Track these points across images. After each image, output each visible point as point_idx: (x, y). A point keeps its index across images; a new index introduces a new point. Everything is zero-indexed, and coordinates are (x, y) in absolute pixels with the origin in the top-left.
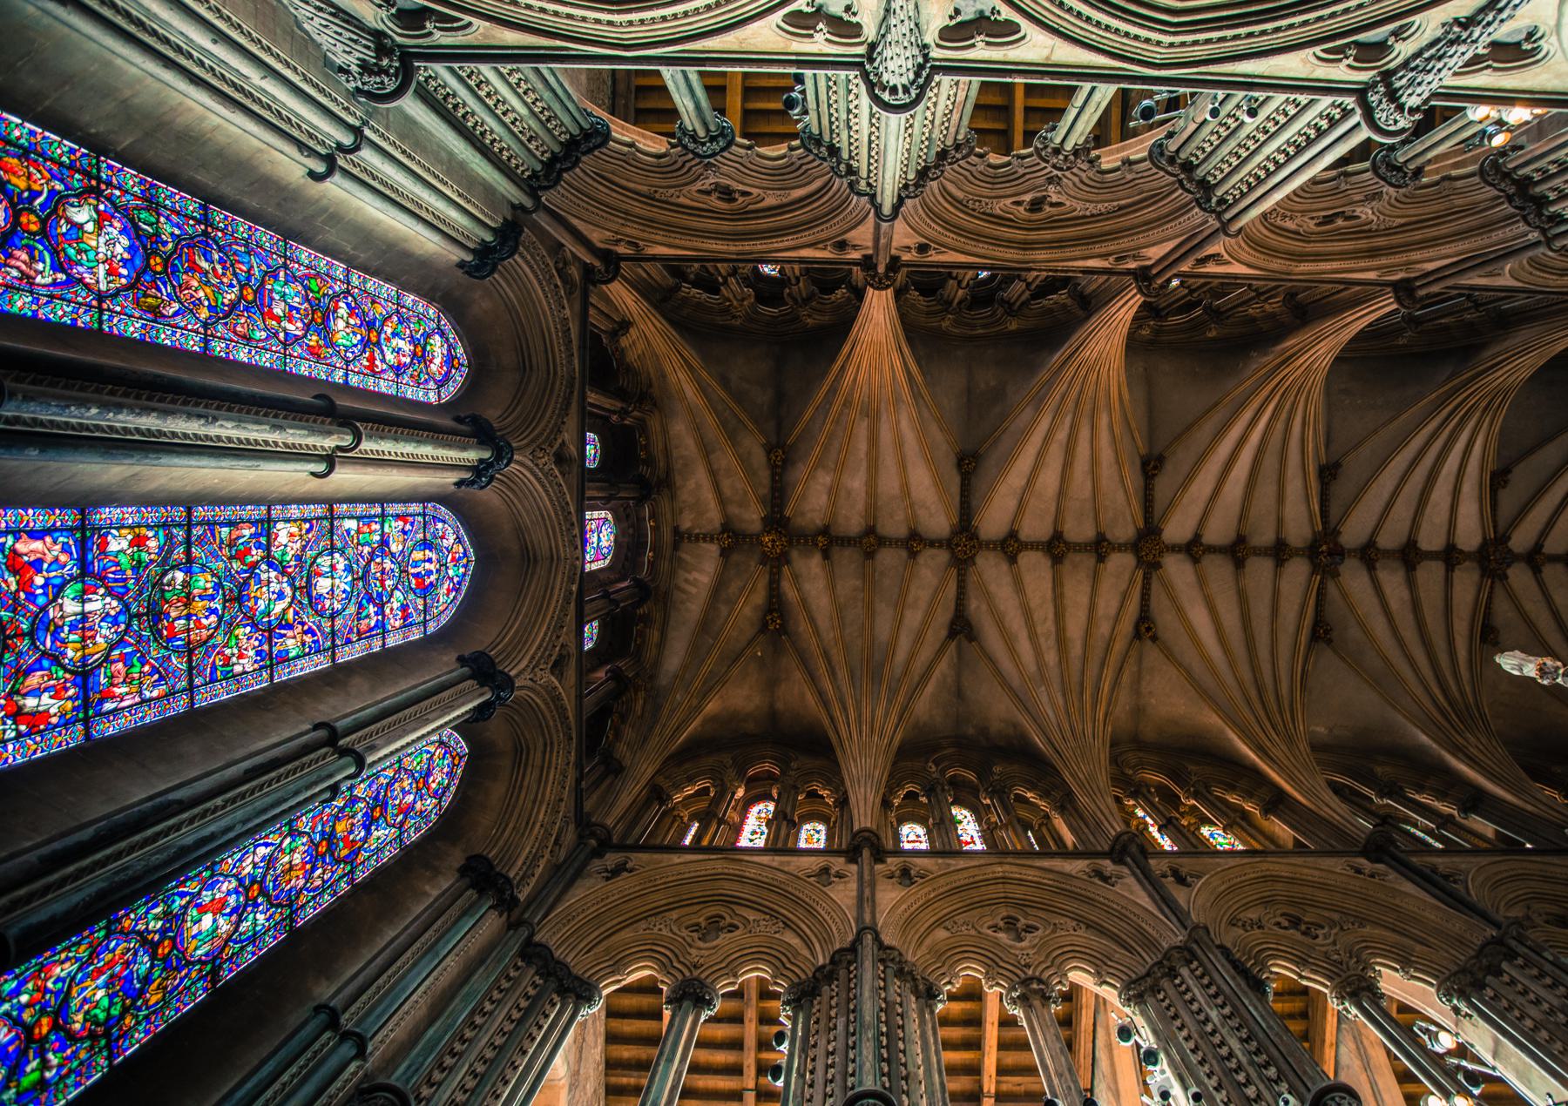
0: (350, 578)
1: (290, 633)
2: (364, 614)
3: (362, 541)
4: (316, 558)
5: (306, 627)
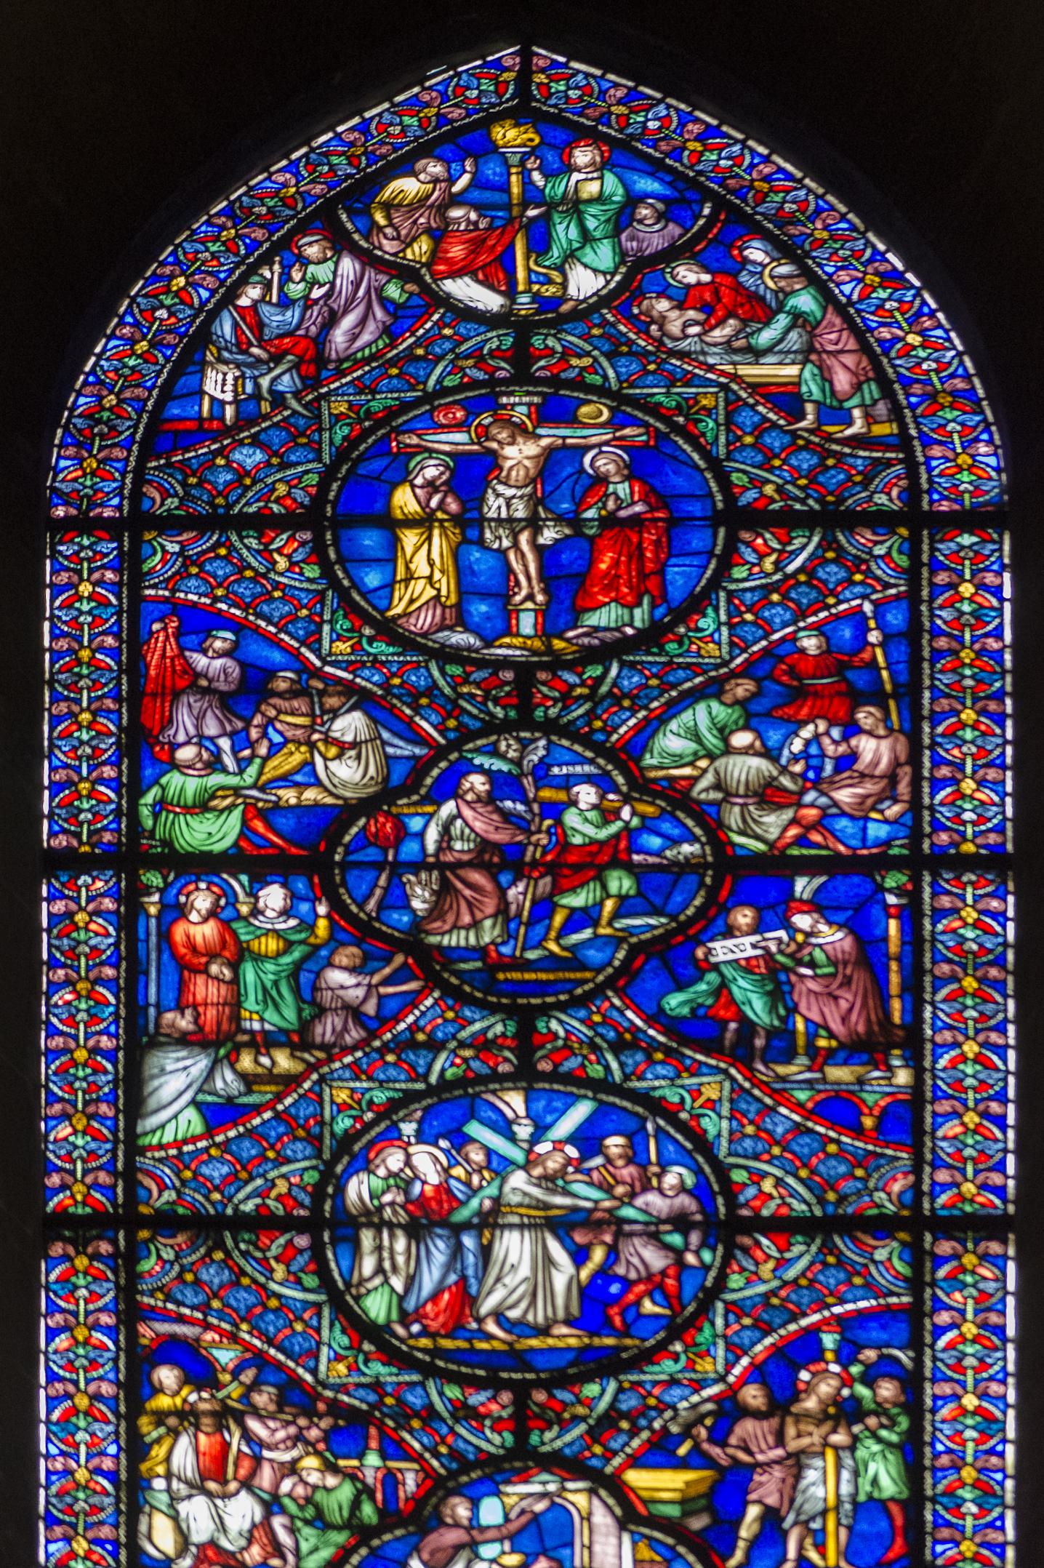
0: (514, 1102)
1: (767, 1488)
2: (757, 1007)
3: (290, 1014)
4: (360, 1328)
5: (753, 1395)
